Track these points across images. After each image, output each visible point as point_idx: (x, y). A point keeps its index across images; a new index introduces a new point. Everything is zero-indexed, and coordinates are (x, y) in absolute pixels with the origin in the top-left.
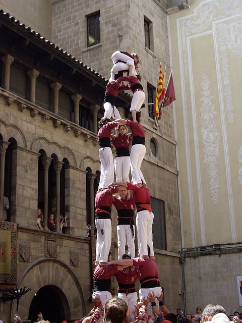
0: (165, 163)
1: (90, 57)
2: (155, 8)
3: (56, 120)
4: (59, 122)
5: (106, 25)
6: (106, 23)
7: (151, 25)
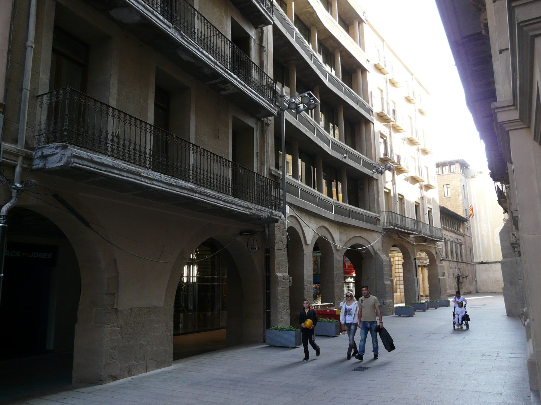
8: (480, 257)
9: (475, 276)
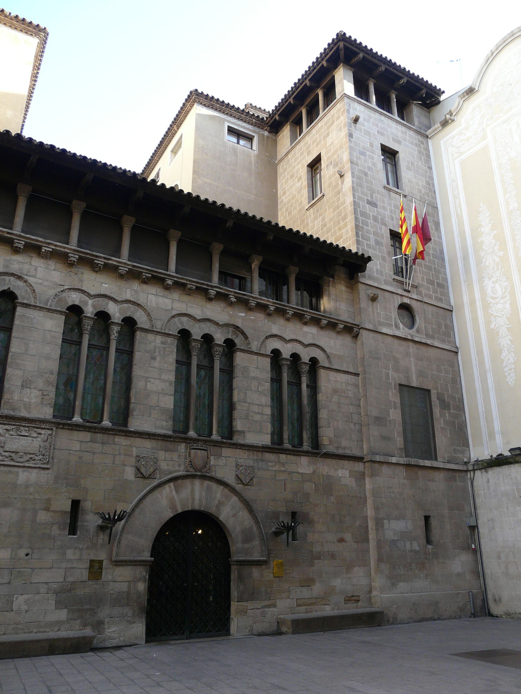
0: (432, 337)
1: (314, 213)
2: (403, 132)
3: (208, 289)
4: (212, 292)
5: (327, 169)
6: (327, 166)
7: (397, 156)
8: (492, 435)
9: (474, 528)
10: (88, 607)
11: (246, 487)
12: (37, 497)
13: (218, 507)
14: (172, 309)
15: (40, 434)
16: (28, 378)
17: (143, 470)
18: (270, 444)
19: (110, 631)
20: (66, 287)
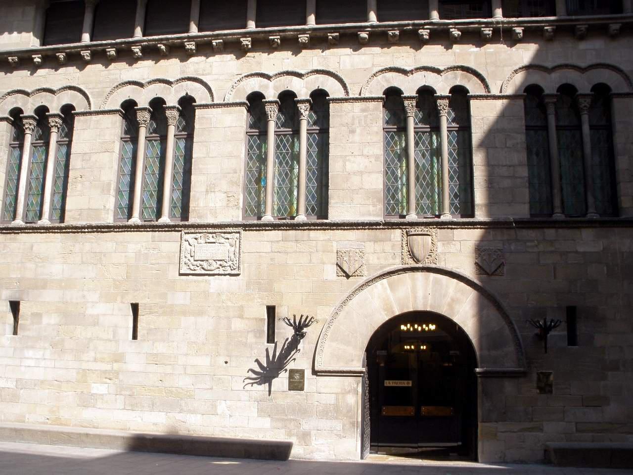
10: (292, 417)
11: (493, 277)
12: (229, 304)
13: (451, 306)
14: (373, 65)
15: (228, 239)
16: (212, 181)
17: (346, 268)
18: (529, 216)
19: (317, 443)
20: (243, 75)
